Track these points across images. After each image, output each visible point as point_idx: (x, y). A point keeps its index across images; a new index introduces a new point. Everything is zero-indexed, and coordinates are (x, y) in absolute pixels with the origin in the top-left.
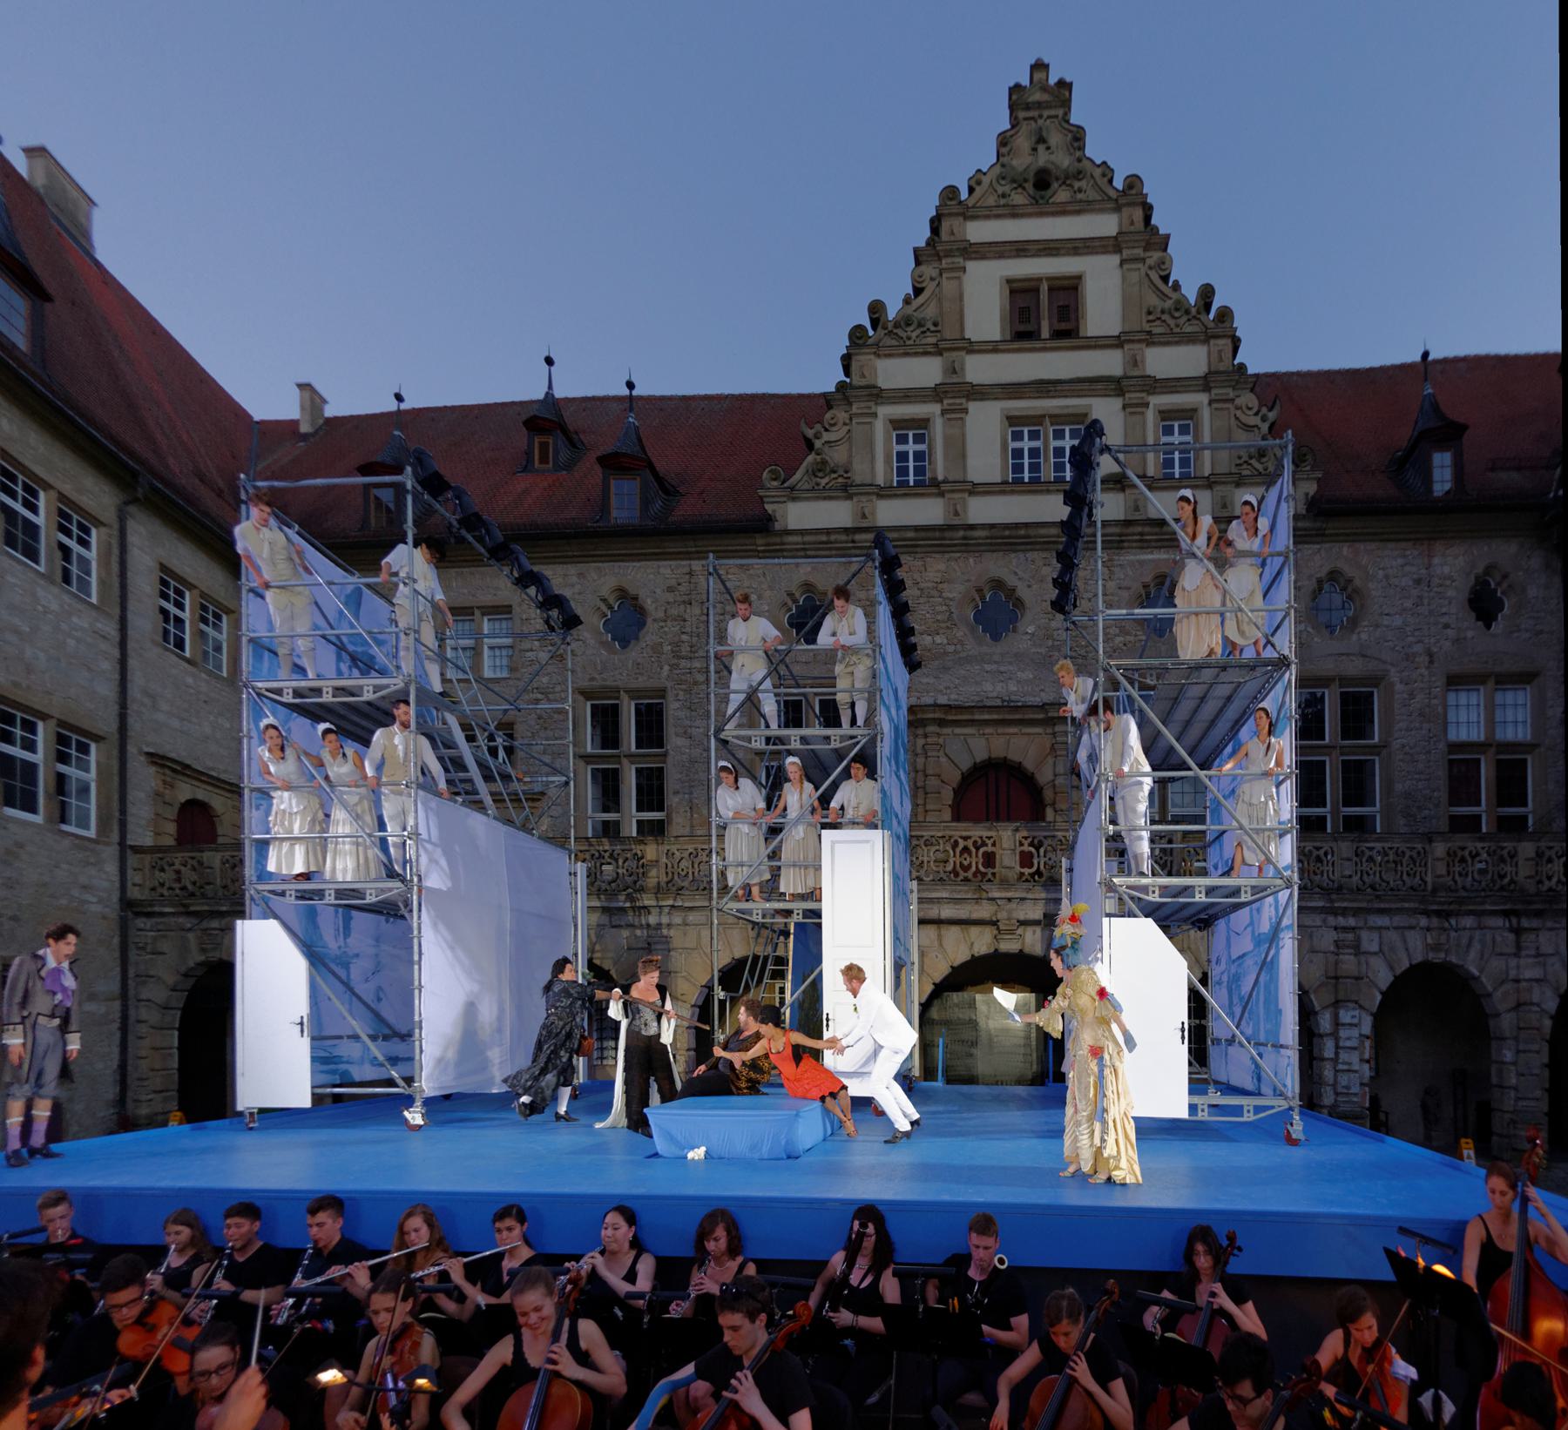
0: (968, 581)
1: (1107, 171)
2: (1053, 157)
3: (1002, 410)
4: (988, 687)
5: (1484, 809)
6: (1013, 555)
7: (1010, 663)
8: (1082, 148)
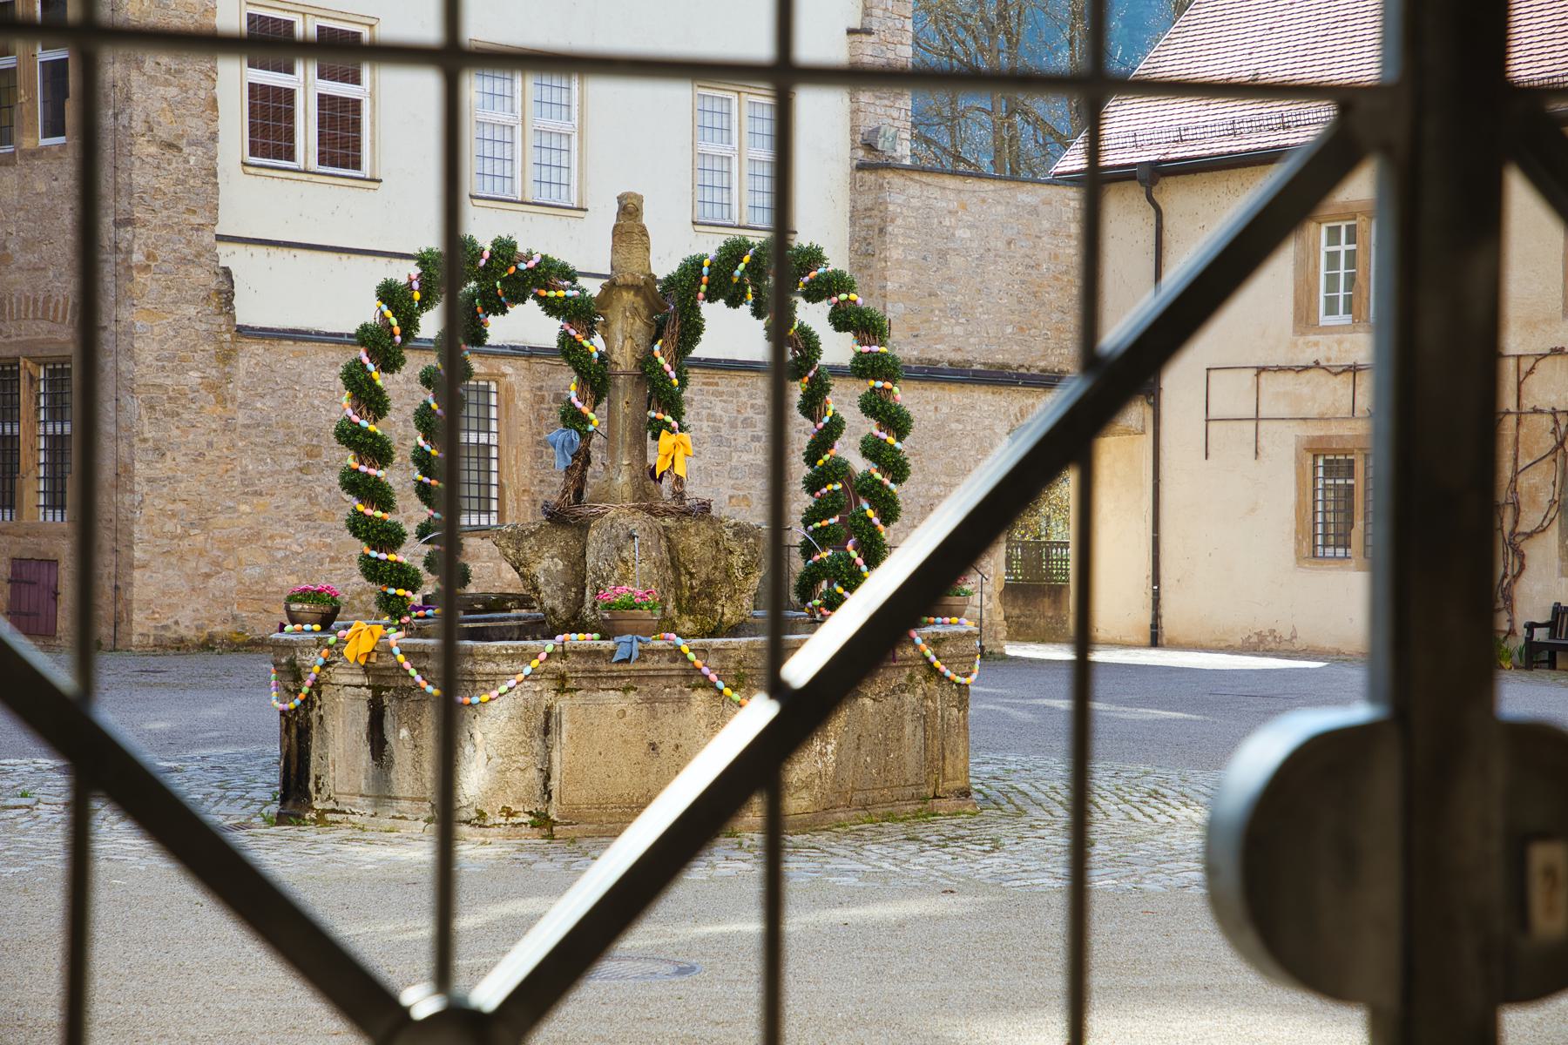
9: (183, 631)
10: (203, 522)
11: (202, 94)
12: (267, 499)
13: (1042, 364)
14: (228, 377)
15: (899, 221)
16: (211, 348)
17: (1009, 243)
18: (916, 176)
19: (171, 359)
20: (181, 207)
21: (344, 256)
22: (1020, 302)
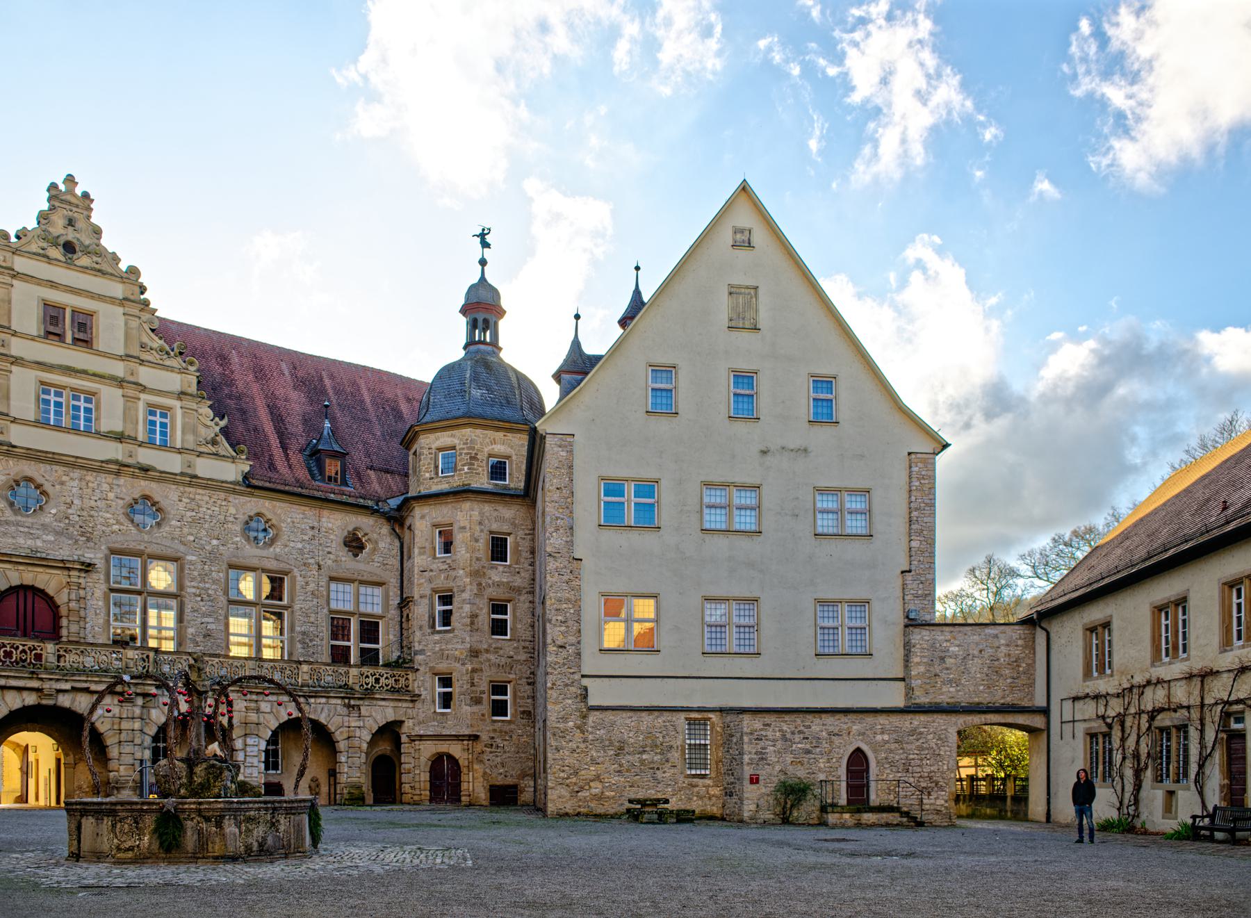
0: (9, 474)
1: (115, 259)
2: (78, 236)
3: (36, 376)
4: (21, 541)
5: (353, 644)
6: (41, 465)
7: (38, 529)
8: (99, 239)
9: (567, 810)
10: (576, 773)
11: (575, 628)
12: (602, 765)
13: (1002, 701)
14: (585, 724)
15: (918, 646)
16: (578, 714)
17: (981, 651)
18: (927, 628)
19: (561, 718)
20: (566, 667)
21: (642, 679)
22: (987, 675)
